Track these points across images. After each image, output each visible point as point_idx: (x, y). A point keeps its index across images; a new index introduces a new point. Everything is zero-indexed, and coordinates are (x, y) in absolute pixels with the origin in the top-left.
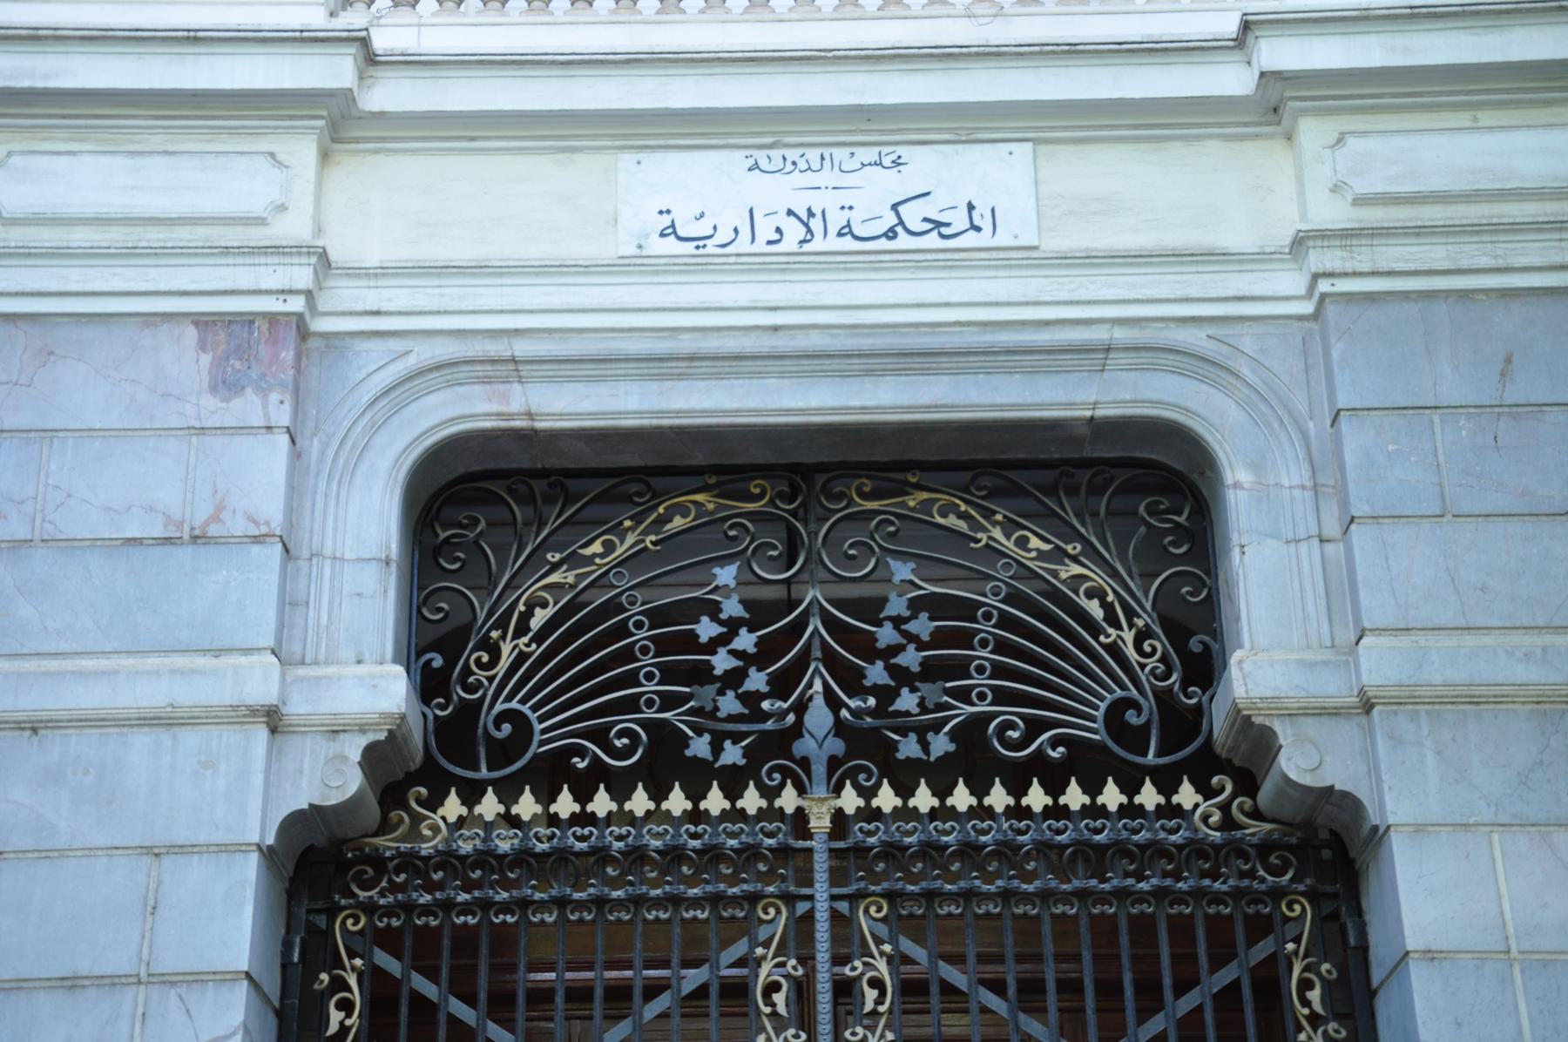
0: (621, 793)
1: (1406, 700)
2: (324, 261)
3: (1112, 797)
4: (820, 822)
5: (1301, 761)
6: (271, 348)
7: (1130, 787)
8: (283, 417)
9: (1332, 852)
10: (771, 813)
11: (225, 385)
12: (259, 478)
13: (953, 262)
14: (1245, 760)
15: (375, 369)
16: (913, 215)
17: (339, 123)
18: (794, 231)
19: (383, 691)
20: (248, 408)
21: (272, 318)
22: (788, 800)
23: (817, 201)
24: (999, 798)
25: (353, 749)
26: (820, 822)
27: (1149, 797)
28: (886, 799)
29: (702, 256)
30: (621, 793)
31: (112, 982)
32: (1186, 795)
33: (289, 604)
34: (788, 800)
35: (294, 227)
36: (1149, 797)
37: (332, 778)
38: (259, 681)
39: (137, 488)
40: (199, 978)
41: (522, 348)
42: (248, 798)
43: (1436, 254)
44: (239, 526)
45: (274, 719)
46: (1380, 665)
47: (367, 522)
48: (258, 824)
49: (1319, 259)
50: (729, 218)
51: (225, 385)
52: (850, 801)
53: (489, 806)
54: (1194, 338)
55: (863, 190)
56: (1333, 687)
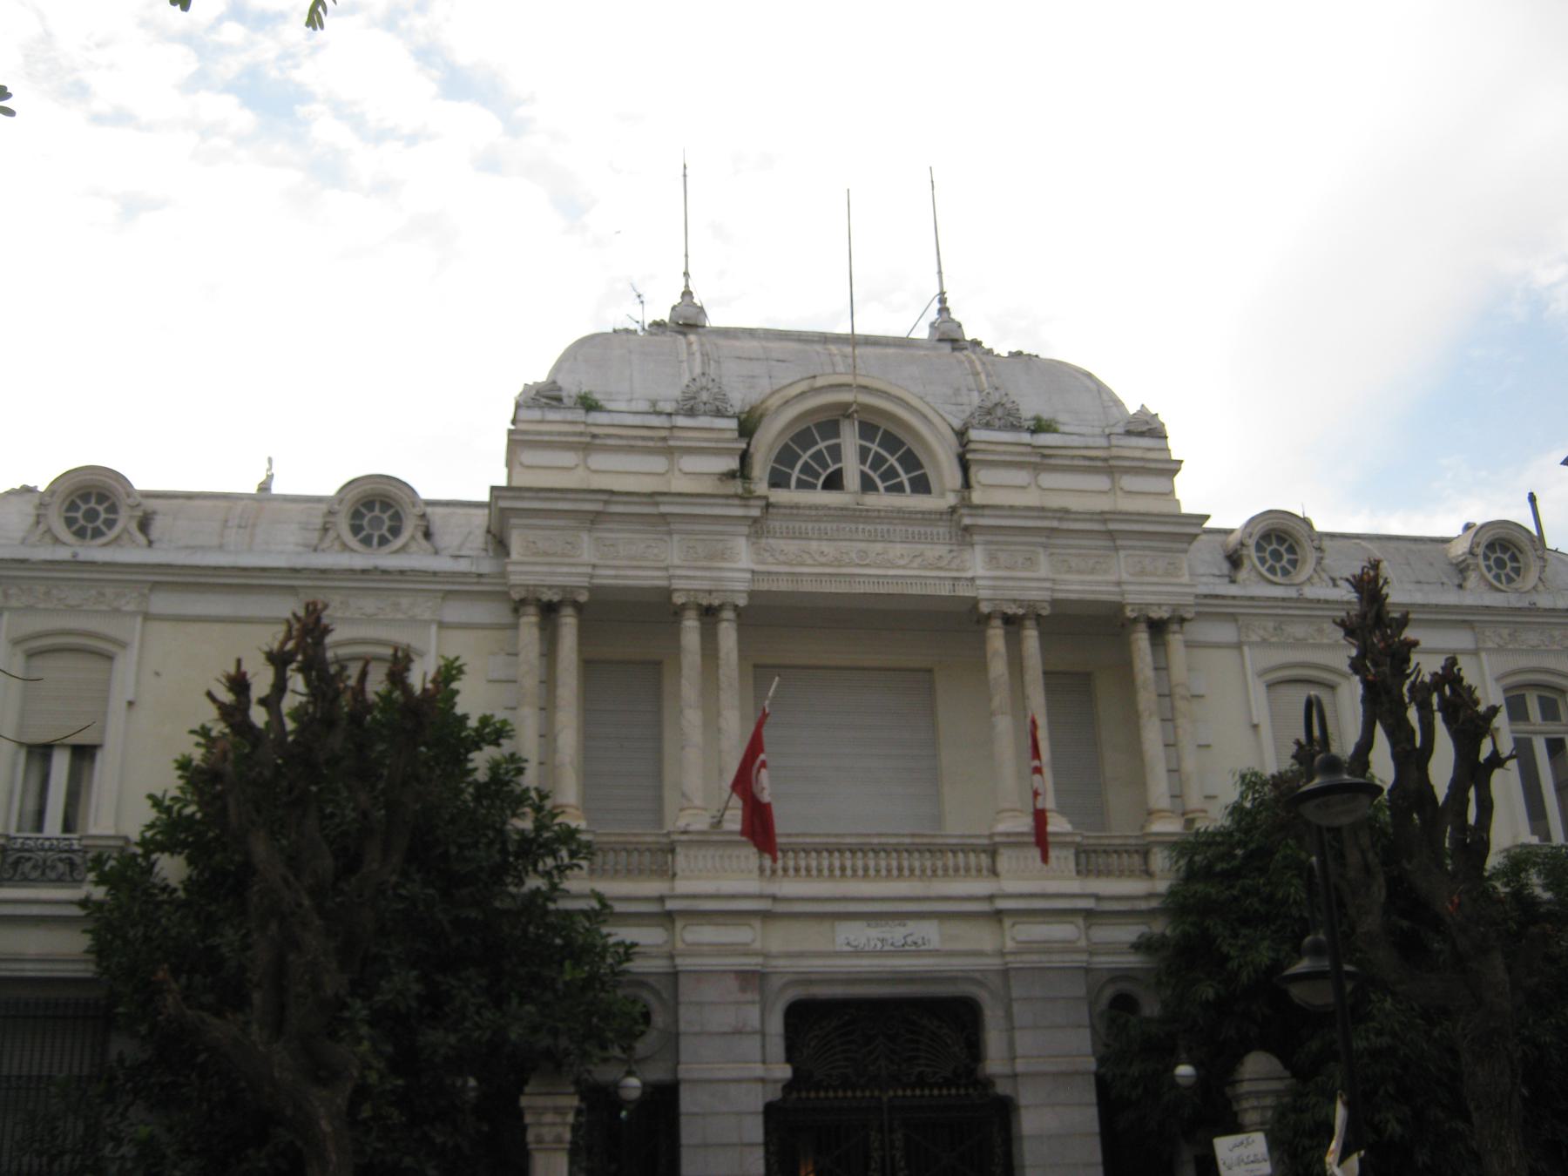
0: (835, 1091)
1: (1025, 1075)
2: (767, 955)
3: (953, 1091)
4: (885, 1099)
5: (1002, 1088)
6: (752, 980)
7: (958, 1088)
8: (757, 998)
9: (1005, 1109)
10: (872, 1097)
11: (743, 990)
12: (753, 1016)
13: (918, 954)
14: (988, 1083)
15: (776, 982)
16: (909, 940)
17: (766, 916)
18: (879, 945)
19: (784, 1072)
20: (749, 996)
21: (754, 972)
22: (877, 1093)
23: (888, 936)
24: (927, 1092)
25: (780, 1086)
26: (885, 1099)
27: (962, 1091)
28: (900, 1093)
29: (858, 953)
30: (835, 1091)
31: (734, 1145)
32: (971, 1091)
33: (763, 1047)
34: (877, 1093)
35: (757, 945)
36: (962, 1091)
37: (775, 1094)
38: (758, 1070)
39: (722, 1019)
40: (752, 1145)
41: (813, 977)
42: (756, 1099)
43: (1035, 958)
44: (749, 1029)
45: (762, 1080)
46: (1020, 1066)
47: (776, 1025)
48: (760, 1108)
49: (1009, 958)
50: (863, 941)
51: (743, 990)
52: (891, 1093)
53: (804, 1094)
54: (978, 975)
55: (896, 933)
56: (1007, 1070)
